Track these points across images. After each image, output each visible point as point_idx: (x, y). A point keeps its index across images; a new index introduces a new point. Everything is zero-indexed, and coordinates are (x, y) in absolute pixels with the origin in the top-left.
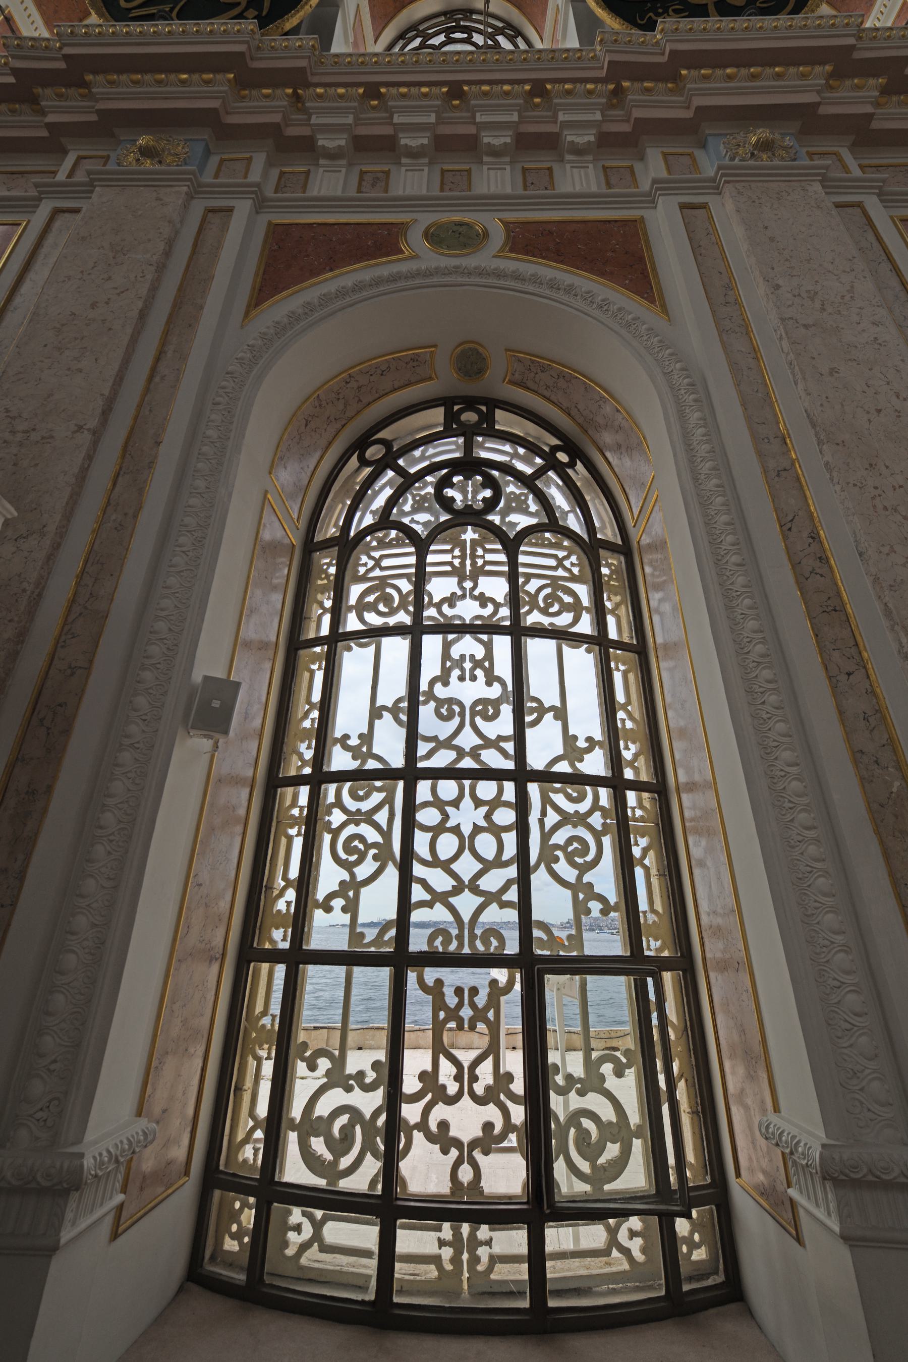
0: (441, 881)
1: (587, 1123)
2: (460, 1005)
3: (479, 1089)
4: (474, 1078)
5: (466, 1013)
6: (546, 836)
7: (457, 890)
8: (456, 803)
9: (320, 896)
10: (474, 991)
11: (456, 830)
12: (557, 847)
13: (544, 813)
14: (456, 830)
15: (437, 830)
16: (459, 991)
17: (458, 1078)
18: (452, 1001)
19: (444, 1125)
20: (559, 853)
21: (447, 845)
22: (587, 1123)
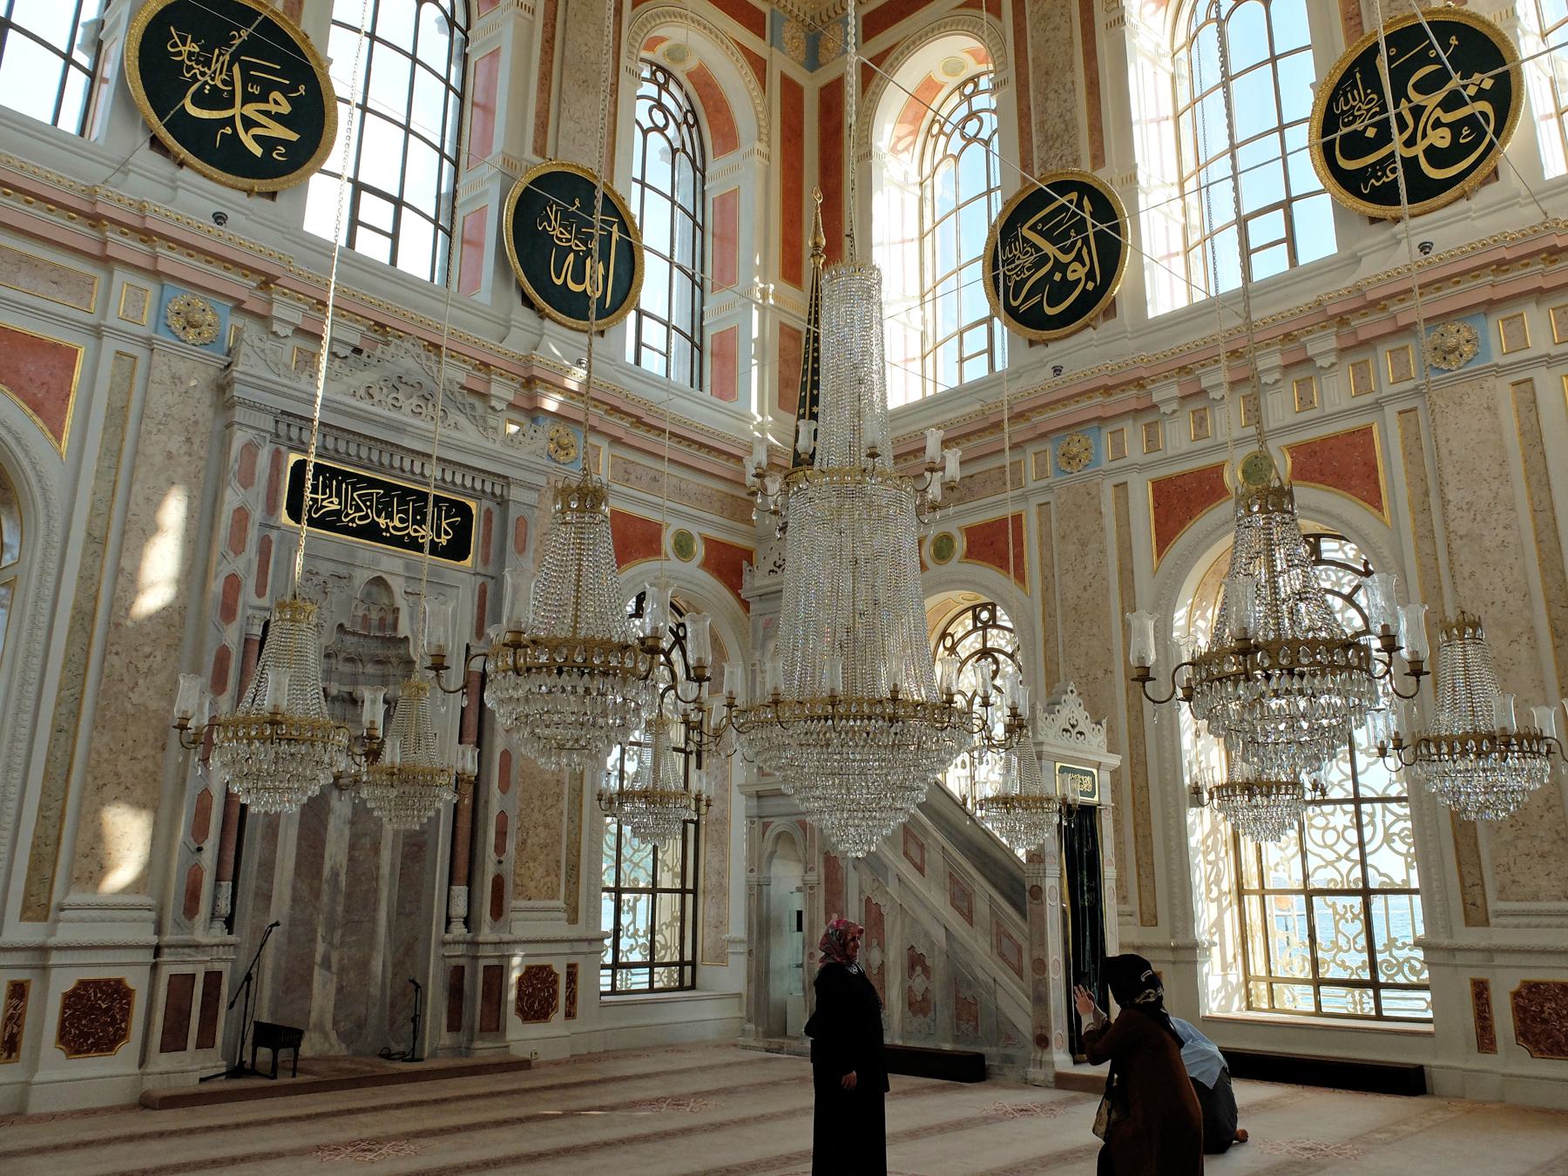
0: (1331, 856)
1: (1413, 962)
2: (1346, 912)
3: (1359, 947)
4: (1355, 943)
5: (1349, 916)
6: (1386, 829)
7: (1339, 859)
8: (1332, 814)
9: (1272, 864)
10: (1352, 907)
11: (1334, 828)
12: (1394, 834)
13: (1384, 816)
14: (1334, 828)
15: (1325, 829)
16: (1345, 907)
17: (1348, 942)
18: (1341, 910)
19: (1343, 961)
20: (1396, 838)
21: (1331, 837)
22: (1413, 962)
